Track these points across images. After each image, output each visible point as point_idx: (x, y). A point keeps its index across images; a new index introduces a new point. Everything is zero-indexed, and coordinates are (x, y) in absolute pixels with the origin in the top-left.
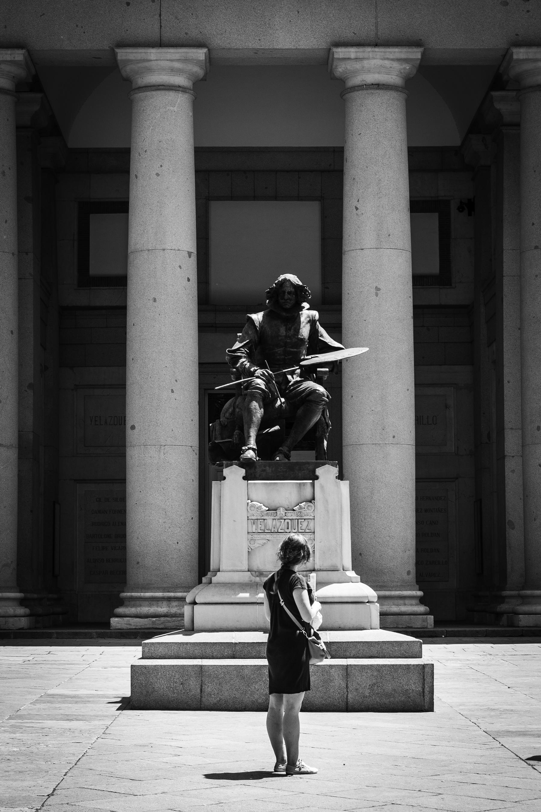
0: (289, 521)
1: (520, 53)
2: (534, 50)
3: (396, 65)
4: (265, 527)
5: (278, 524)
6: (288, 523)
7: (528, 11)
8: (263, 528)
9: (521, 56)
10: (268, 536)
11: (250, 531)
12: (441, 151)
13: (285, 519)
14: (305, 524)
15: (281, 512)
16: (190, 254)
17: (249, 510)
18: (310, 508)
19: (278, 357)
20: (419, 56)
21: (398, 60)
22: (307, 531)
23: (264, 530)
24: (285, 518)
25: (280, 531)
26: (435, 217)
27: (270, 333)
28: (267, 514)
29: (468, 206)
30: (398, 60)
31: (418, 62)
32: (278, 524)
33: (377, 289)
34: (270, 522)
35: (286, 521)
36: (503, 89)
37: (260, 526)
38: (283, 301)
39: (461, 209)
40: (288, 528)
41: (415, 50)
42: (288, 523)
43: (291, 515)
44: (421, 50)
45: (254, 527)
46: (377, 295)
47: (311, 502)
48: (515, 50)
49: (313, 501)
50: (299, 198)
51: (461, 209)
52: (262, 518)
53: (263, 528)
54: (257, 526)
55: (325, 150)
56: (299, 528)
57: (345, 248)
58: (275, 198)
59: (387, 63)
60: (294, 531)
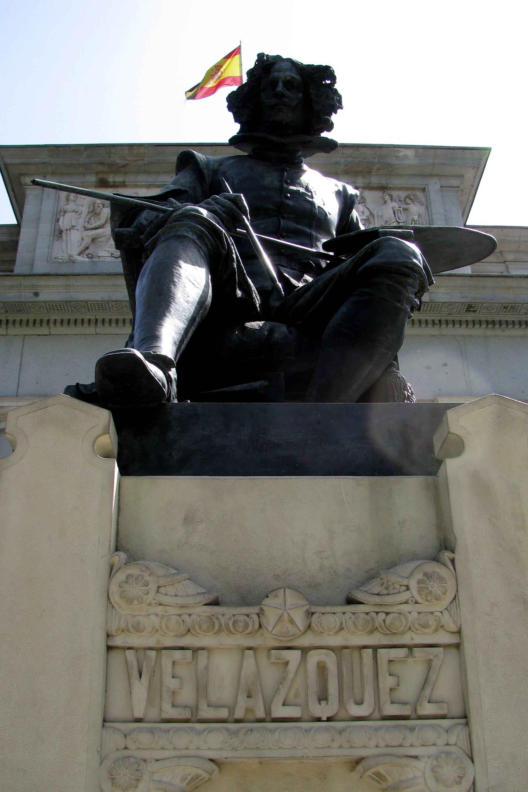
0: (331, 660)
4: (202, 687)
5: (270, 675)
6: (322, 668)
7: (447, 373)
8: (187, 696)
10: (214, 742)
11: (117, 710)
13: (305, 651)
14: (412, 673)
15: (285, 612)
17: (115, 598)
18: (435, 587)
22: (428, 709)
23: (196, 709)
24: (306, 641)
25: (280, 712)
28: (213, 626)
32: (270, 675)
34: (224, 669)
35: (314, 658)
37: (171, 683)
38: (273, 101)
40: (323, 697)
42: (322, 668)
43: (341, 629)
45: (140, 689)
47: (436, 559)
49: (446, 555)
52: (187, 641)
53: (187, 696)
54: (154, 694)
56: (385, 697)
60: (355, 711)
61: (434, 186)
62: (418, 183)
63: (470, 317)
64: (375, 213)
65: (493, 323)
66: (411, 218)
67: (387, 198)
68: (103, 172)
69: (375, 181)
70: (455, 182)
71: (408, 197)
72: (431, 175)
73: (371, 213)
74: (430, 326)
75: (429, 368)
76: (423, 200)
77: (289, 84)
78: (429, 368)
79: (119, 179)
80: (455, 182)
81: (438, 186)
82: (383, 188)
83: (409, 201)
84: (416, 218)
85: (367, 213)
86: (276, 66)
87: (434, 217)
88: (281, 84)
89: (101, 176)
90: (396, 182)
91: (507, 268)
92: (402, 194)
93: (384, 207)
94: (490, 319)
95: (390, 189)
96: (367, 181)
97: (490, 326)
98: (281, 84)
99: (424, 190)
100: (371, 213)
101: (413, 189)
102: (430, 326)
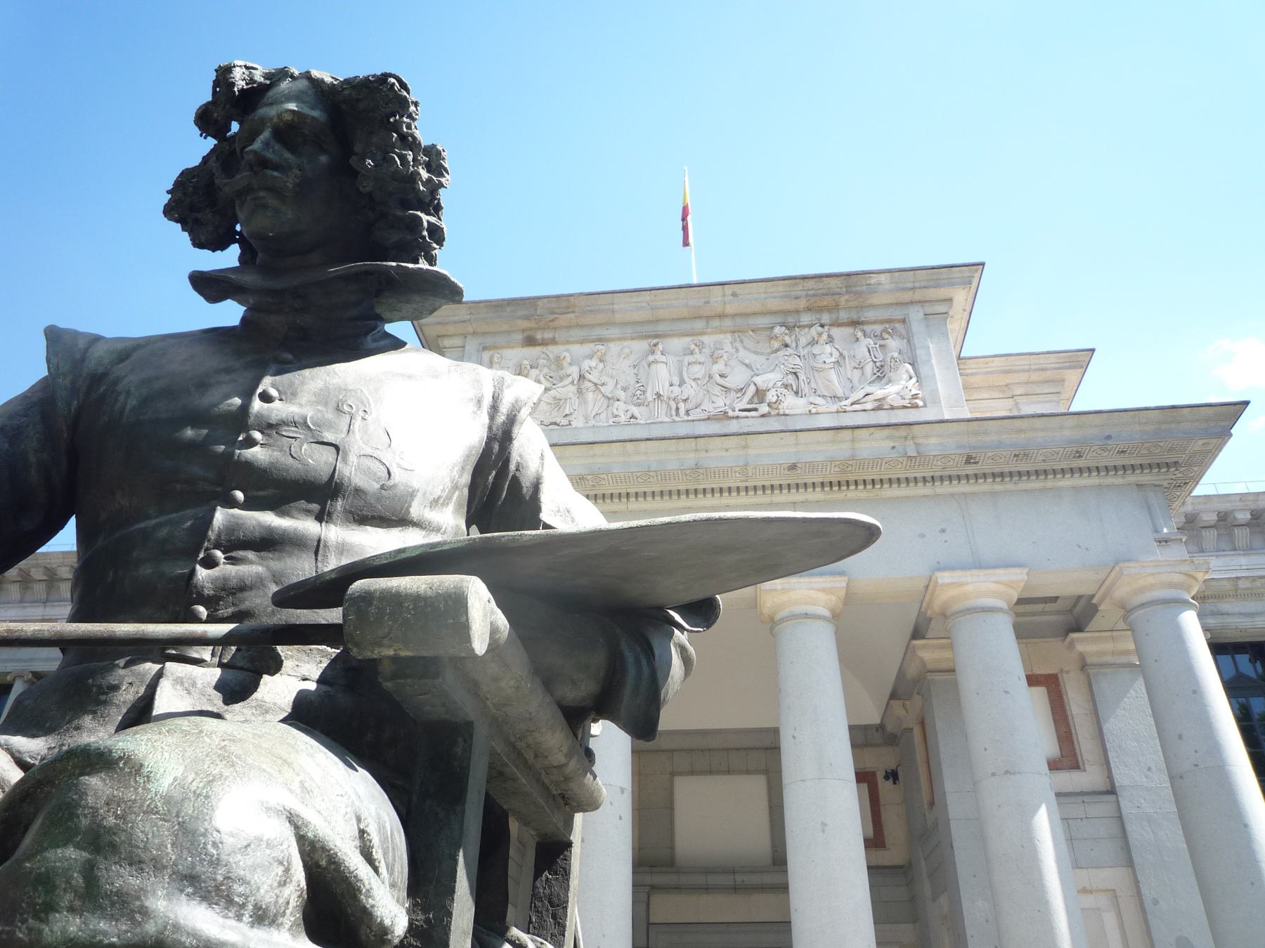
1: (944, 577)
2: (958, 573)
3: (823, 597)
9: (947, 581)
12: (866, 728)
16: (622, 790)
19: (146, 570)
20: (844, 584)
21: (824, 590)
26: (865, 785)
27: (133, 402)
29: (893, 776)
30: (824, 590)
31: (843, 592)
33: (824, 824)
36: (923, 638)
39: (886, 777)
41: (839, 578)
44: (846, 578)
46: (823, 831)
48: (938, 574)
50: (748, 772)
51: (886, 777)
55: (767, 730)
57: (786, 781)
58: (728, 772)
59: (813, 594)
61: (916, 314)
62: (897, 313)
63: (970, 470)
64: (845, 353)
65: (1002, 475)
66: (890, 355)
67: (859, 334)
68: (531, 329)
69: (844, 316)
70: (941, 308)
71: (885, 330)
72: (912, 303)
73: (841, 354)
74: (920, 484)
75: (922, 536)
76: (904, 332)
77: (288, 132)
78: (922, 536)
79: (548, 335)
80: (941, 308)
81: (921, 315)
82: (855, 323)
83: (886, 336)
84: (896, 355)
85: (836, 354)
86: (271, 93)
87: (918, 352)
88: (266, 134)
89: (528, 333)
90: (870, 315)
91: (1017, 404)
92: (878, 328)
93: (856, 345)
94: (997, 470)
95: (862, 323)
96: (834, 316)
97: (998, 479)
98: (266, 134)
99: (904, 321)
100: (841, 354)
101: (890, 321)
102: (920, 484)
